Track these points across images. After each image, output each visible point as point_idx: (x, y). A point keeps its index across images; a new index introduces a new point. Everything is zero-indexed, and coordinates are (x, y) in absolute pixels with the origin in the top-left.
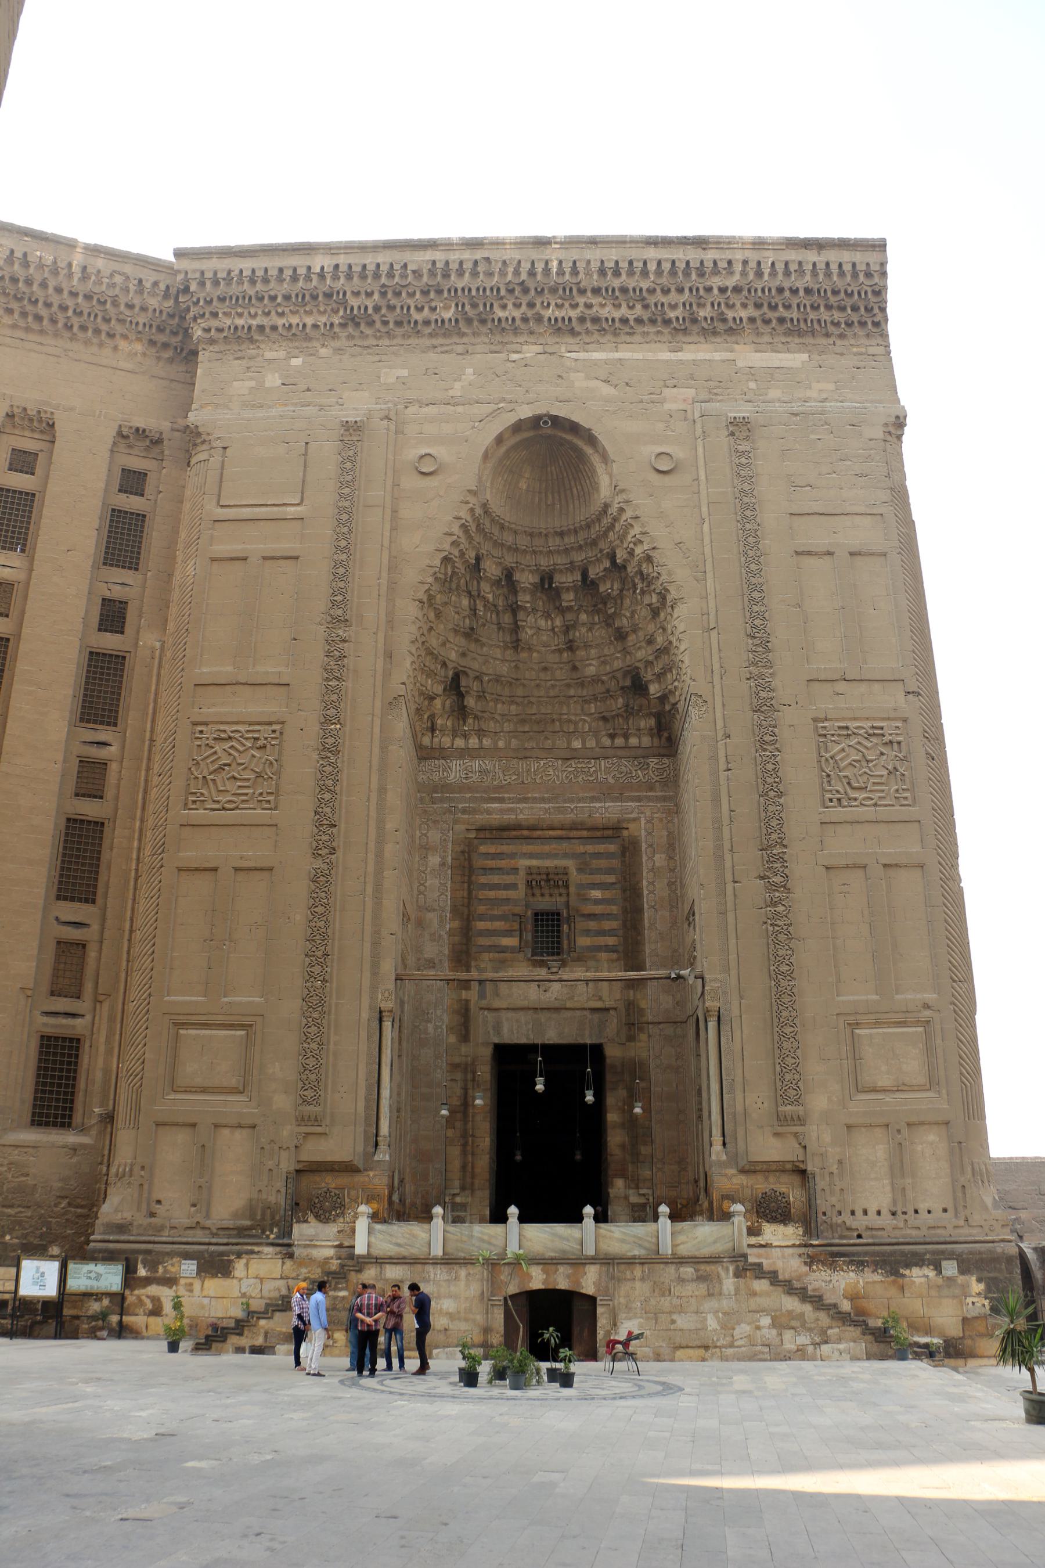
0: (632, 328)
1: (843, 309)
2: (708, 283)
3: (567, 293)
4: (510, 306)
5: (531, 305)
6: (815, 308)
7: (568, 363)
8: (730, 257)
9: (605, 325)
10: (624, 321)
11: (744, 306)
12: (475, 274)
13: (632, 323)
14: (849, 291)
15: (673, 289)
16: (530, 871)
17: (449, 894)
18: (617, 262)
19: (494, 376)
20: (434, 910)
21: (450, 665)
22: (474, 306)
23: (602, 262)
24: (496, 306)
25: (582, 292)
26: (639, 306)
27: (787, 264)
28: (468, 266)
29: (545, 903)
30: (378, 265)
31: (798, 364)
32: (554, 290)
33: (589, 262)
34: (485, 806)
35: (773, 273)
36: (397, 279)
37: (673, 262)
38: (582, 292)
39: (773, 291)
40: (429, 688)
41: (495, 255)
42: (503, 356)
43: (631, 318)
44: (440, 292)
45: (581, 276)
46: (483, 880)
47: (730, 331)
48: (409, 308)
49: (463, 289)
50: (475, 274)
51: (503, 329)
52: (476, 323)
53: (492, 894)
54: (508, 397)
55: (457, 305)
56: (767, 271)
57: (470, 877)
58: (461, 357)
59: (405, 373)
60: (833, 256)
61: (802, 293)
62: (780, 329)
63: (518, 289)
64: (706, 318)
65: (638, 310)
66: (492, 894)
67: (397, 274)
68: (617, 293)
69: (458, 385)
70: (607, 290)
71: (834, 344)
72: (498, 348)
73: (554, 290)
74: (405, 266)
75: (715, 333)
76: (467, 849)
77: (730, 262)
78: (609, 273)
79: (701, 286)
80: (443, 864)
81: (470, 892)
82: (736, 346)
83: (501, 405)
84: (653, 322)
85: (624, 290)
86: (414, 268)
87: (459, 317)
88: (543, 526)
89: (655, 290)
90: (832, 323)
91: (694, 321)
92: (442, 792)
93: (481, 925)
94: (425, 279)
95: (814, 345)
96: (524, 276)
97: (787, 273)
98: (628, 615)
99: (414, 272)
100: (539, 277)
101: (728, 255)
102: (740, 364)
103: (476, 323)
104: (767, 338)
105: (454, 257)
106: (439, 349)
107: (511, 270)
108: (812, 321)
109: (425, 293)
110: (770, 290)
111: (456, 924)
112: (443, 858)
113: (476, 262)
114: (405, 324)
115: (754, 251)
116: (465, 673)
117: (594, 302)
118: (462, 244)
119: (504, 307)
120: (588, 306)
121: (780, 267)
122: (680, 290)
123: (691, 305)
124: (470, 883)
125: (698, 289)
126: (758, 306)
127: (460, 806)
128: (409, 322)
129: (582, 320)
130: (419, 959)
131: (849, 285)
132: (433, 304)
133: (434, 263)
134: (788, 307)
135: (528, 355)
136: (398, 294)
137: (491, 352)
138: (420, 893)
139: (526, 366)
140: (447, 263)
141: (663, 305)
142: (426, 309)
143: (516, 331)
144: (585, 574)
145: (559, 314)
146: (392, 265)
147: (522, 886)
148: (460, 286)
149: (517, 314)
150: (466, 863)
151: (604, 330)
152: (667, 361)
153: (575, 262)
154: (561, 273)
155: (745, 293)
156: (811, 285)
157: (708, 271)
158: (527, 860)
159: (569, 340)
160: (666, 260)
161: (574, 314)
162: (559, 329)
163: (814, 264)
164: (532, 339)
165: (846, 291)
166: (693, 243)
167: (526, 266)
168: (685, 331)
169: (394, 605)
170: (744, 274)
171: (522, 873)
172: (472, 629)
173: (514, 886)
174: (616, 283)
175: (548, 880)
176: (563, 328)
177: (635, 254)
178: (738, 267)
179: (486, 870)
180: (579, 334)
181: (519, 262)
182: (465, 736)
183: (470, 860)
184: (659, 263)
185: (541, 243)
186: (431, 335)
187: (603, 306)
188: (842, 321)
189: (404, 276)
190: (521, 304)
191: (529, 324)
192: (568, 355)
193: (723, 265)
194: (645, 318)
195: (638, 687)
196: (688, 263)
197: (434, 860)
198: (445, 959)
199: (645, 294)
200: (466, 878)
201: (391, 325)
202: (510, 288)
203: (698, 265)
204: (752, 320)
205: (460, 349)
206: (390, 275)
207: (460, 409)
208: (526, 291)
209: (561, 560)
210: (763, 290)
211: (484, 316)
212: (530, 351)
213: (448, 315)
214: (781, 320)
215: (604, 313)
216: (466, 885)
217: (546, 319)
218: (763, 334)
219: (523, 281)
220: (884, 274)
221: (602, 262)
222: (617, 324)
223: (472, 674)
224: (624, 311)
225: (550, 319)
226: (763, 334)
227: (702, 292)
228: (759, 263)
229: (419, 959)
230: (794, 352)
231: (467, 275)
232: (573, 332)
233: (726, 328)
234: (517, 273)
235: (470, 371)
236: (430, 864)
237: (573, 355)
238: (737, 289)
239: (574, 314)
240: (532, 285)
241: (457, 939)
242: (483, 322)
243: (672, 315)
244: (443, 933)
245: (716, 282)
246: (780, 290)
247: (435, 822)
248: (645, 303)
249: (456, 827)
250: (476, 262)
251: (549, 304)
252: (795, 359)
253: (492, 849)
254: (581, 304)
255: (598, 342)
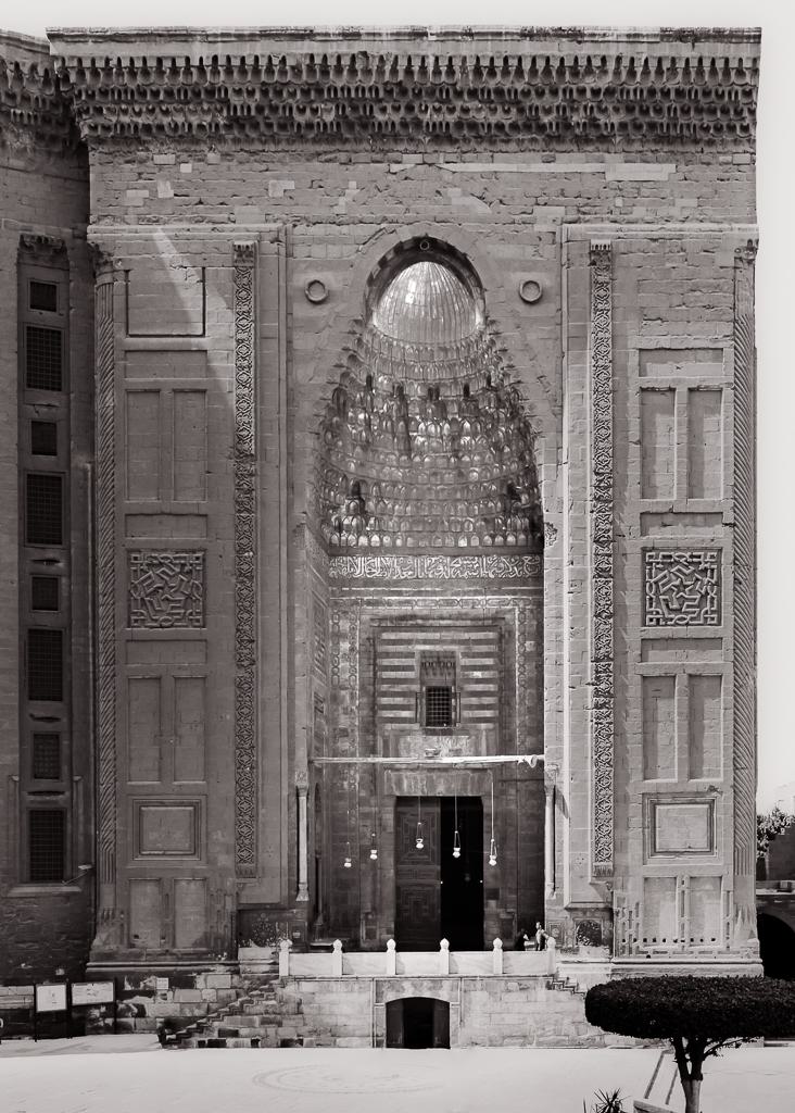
0: (507, 135)
1: (713, 112)
2: (582, 85)
3: (444, 95)
4: (389, 110)
5: (410, 108)
6: (685, 111)
7: (447, 177)
8: (604, 53)
9: (482, 133)
10: (500, 127)
11: (617, 110)
12: (353, 71)
13: (507, 129)
14: (720, 92)
15: (547, 92)
16: (423, 653)
17: (357, 675)
18: (492, 59)
19: (376, 191)
20: (347, 689)
21: (350, 477)
22: (355, 109)
23: (478, 59)
24: (375, 108)
25: (459, 94)
26: (514, 110)
27: (660, 60)
28: (346, 62)
29: (436, 680)
30: (257, 58)
31: (664, 177)
32: (431, 93)
33: (464, 59)
34: (386, 598)
35: (646, 72)
36: (276, 77)
37: (548, 59)
38: (459, 94)
39: (645, 93)
40: (332, 500)
41: (374, 49)
42: (384, 166)
43: (507, 123)
44: (320, 91)
45: (458, 75)
46: (386, 662)
47: (603, 139)
48: (291, 109)
49: (342, 89)
50: (353, 71)
51: (384, 136)
52: (357, 128)
53: (392, 674)
54: (390, 216)
55: (337, 107)
56: (639, 70)
57: (375, 660)
58: (344, 167)
59: (291, 185)
60: (706, 49)
61: (672, 95)
62: (650, 136)
63: (396, 90)
64: (578, 124)
65: (514, 115)
66: (392, 674)
67: (276, 69)
68: (493, 97)
69: (342, 201)
70: (482, 90)
71: (702, 152)
72: (378, 157)
73: (431, 93)
74: (284, 59)
75: (588, 141)
76: (371, 636)
77: (604, 59)
78: (485, 73)
79: (574, 87)
80: (352, 649)
81: (375, 674)
82: (606, 155)
83: (383, 226)
84: (528, 127)
85: (499, 92)
86: (294, 64)
87: (341, 121)
88: (428, 341)
89: (529, 91)
90: (701, 127)
91: (568, 127)
92: (349, 586)
93: (385, 701)
94: (304, 76)
95: (683, 153)
96: (401, 76)
97: (659, 71)
98: (503, 429)
99: (293, 68)
100: (416, 77)
101: (601, 50)
102: (610, 177)
103: (357, 128)
104: (637, 146)
105: (332, 49)
106: (323, 157)
107: (388, 68)
108: (682, 126)
109: (306, 93)
110: (642, 91)
111: (365, 700)
112: (353, 644)
113: (353, 58)
114: (289, 127)
115: (629, 45)
116: (364, 482)
117: (469, 105)
118: (339, 34)
119: (384, 110)
120: (466, 110)
121: (653, 65)
122: (554, 93)
123: (564, 109)
124: (375, 665)
125: (571, 91)
126: (630, 110)
127: (365, 598)
128: (292, 125)
129: (459, 125)
130: (335, 730)
131: (720, 85)
132: (314, 106)
133: (312, 57)
134: (659, 111)
135: (408, 166)
136: (279, 93)
137: (373, 162)
138: (334, 674)
139: (406, 179)
140: (325, 58)
141: (537, 108)
142: (308, 111)
143: (396, 138)
144: (466, 389)
145: (437, 118)
146: (270, 59)
147: (417, 668)
148: (339, 84)
149: (396, 118)
150: (371, 649)
151: (481, 137)
152: (539, 174)
153: (450, 59)
154: (437, 72)
155: (617, 95)
156: (682, 86)
157: (582, 70)
158: (422, 645)
159: (449, 149)
160: (541, 56)
161: (451, 118)
162: (437, 136)
163: (687, 60)
164: (411, 148)
165: (717, 92)
166: (568, 36)
167: (403, 63)
168: (559, 139)
169: (293, 439)
170: (617, 73)
171: (417, 656)
172: (368, 442)
173: (410, 668)
174: (492, 84)
175: (439, 662)
176: (441, 136)
177: (509, 48)
178: (611, 66)
179: (387, 655)
180: (457, 141)
181: (396, 58)
182: (367, 534)
183: (374, 645)
184: (534, 60)
185: (418, 34)
186: (315, 141)
187: (479, 110)
188: (712, 124)
189: (283, 72)
190: (400, 107)
191: (408, 132)
192: (446, 166)
193: (596, 63)
194: (520, 123)
195: (512, 494)
196: (562, 60)
197: (345, 646)
198: (356, 729)
199: (519, 97)
200: (372, 661)
201: (275, 129)
202: (388, 89)
203: (572, 64)
204: (623, 126)
205: (343, 157)
206: (270, 71)
207: (345, 229)
208: (404, 92)
209: (445, 375)
210: (635, 91)
211: (364, 120)
212: (410, 161)
213: (329, 118)
214: (652, 126)
215: (481, 117)
216: (372, 667)
217: (424, 124)
218: (633, 141)
219: (401, 82)
220: (755, 71)
221: (478, 59)
222: (493, 131)
223: (370, 482)
224: (499, 117)
225: (428, 124)
226: (633, 141)
227: (575, 95)
228: (632, 60)
229: (335, 730)
230: (664, 162)
231: (345, 73)
232: (452, 141)
233: (598, 134)
234: (394, 71)
235: (353, 184)
236: (342, 649)
237: (451, 167)
238: (610, 92)
239: (451, 118)
240: (410, 86)
241: (365, 712)
242: (364, 126)
243: (546, 120)
244: (354, 708)
245: (589, 83)
246: (652, 92)
247: (345, 612)
248: (520, 106)
249: (363, 617)
250: (353, 58)
251: (427, 108)
252: (660, 171)
253: (392, 636)
254: (458, 109)
255: (475, 151)
